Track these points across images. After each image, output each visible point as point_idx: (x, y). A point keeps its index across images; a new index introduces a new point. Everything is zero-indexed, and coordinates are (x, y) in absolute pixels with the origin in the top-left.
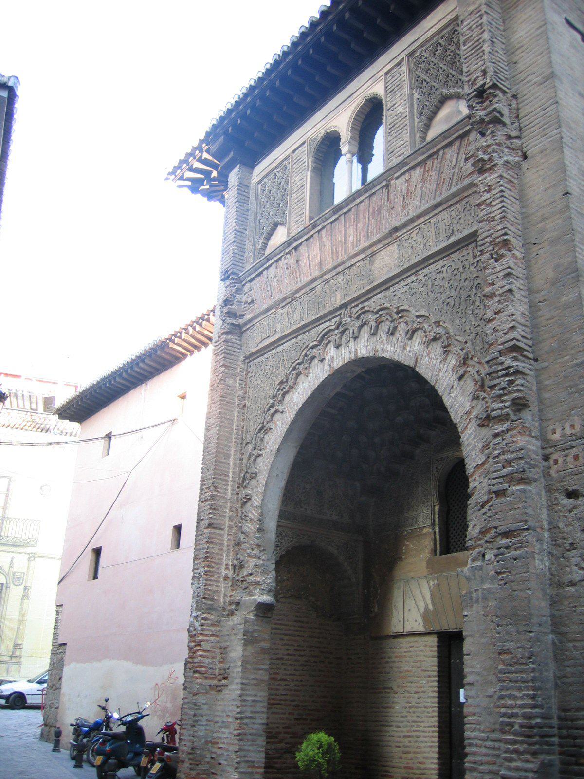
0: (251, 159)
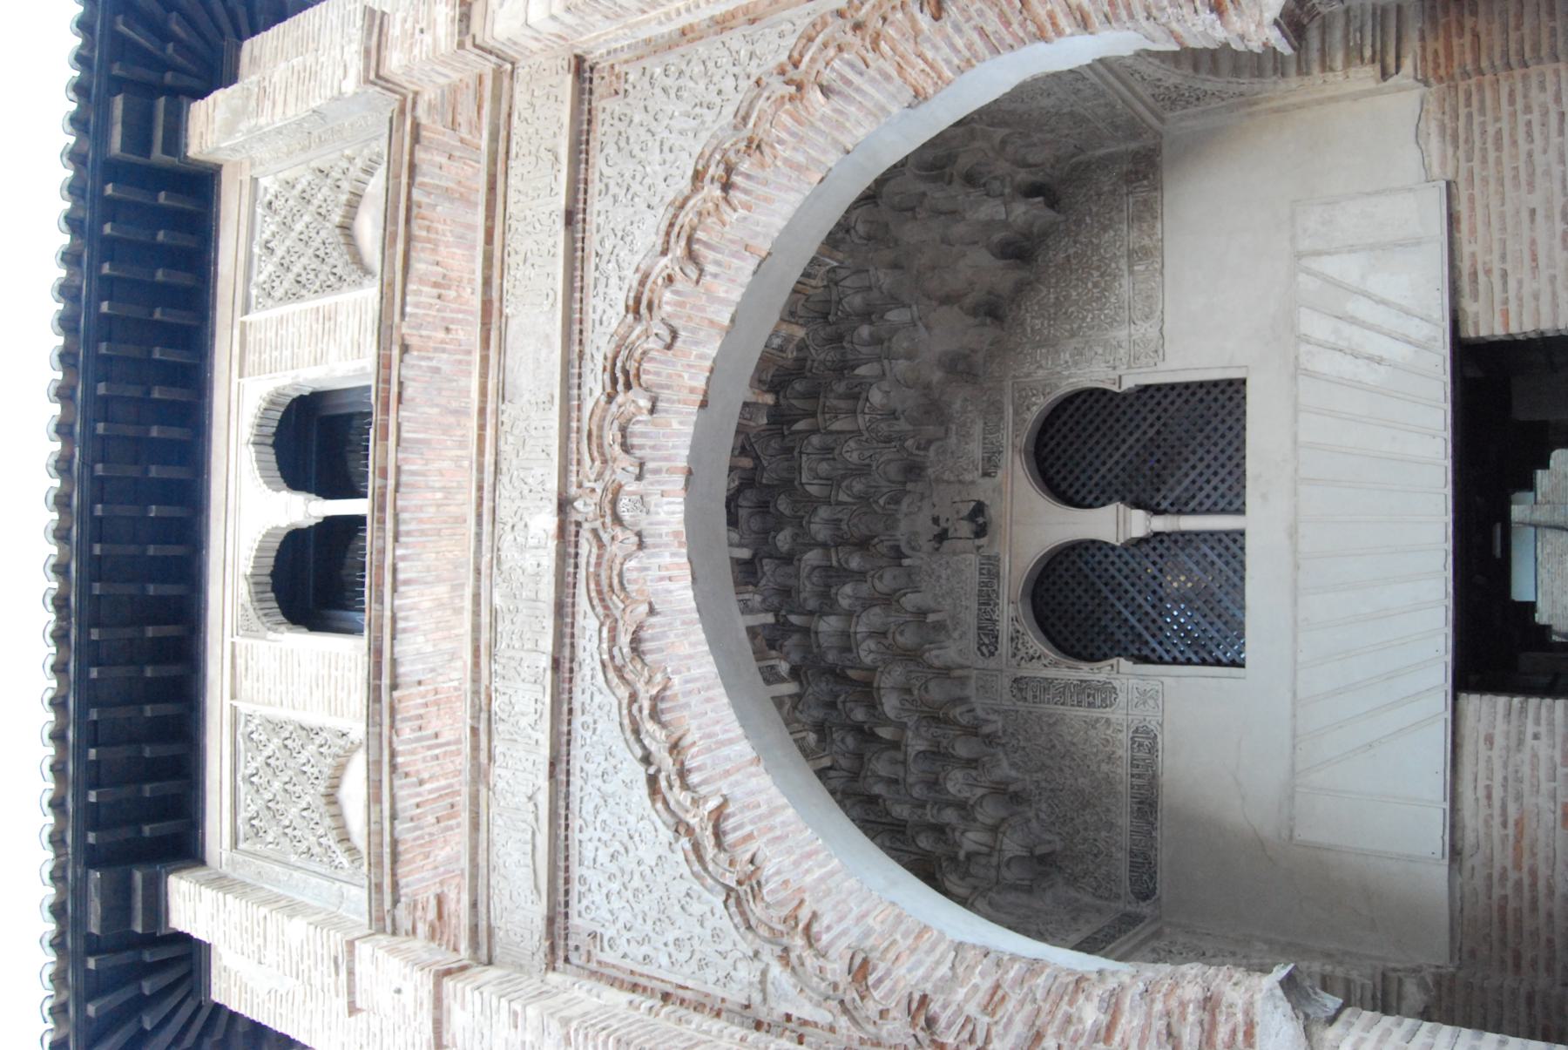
0: (185, 848)
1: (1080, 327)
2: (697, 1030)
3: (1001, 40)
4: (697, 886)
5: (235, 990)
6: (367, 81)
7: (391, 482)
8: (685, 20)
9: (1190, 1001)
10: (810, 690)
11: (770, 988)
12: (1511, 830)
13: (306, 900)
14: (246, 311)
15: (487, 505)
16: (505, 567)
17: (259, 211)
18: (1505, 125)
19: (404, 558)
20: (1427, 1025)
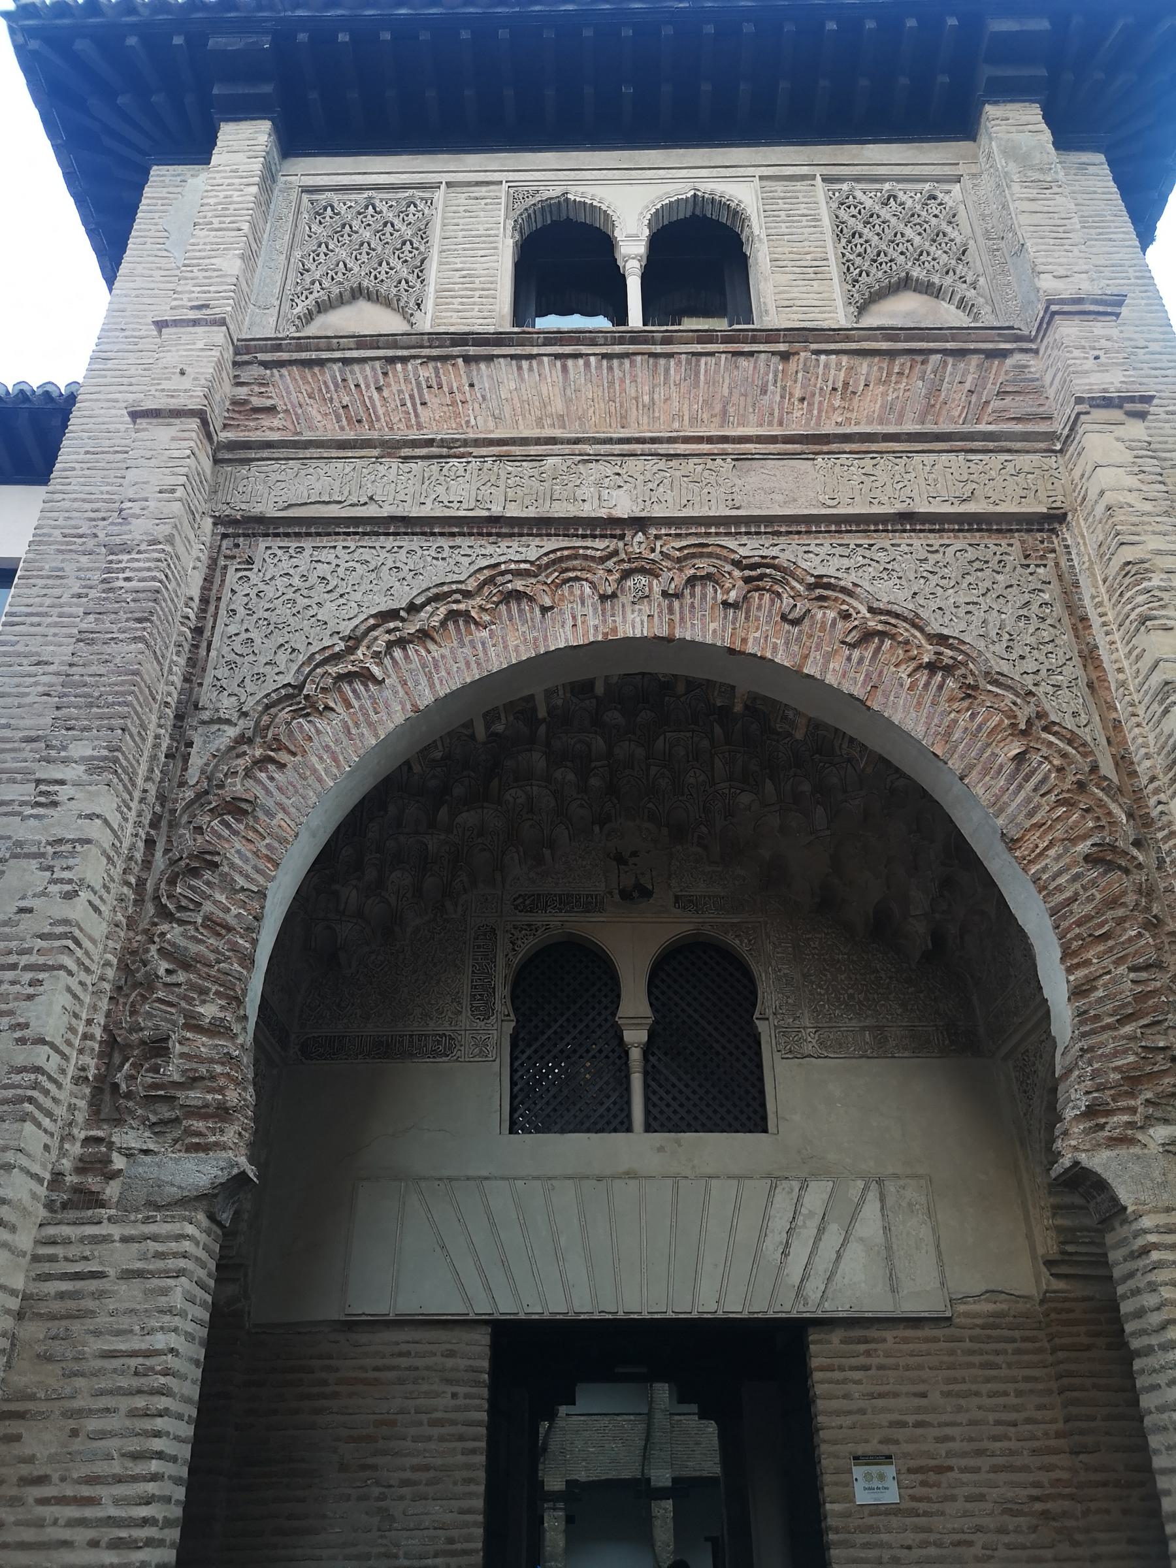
1: (812, 983)
2: (172, 661)
3: (1064, 917)
4: (302, 658)
5: (163, 192)
6: (1050, 302)
7: (658, 349)
8: (1096, 621)
9: (224, 1095)
11: (216, 727)
12: (372, 1375)
13: (258, 271)
14: (826, 179)
15: (638, 448)
16: (580, 466)
17: (927, 186)
18: (1004, 1372)
19: (587, 365)
20: (209, 1299)
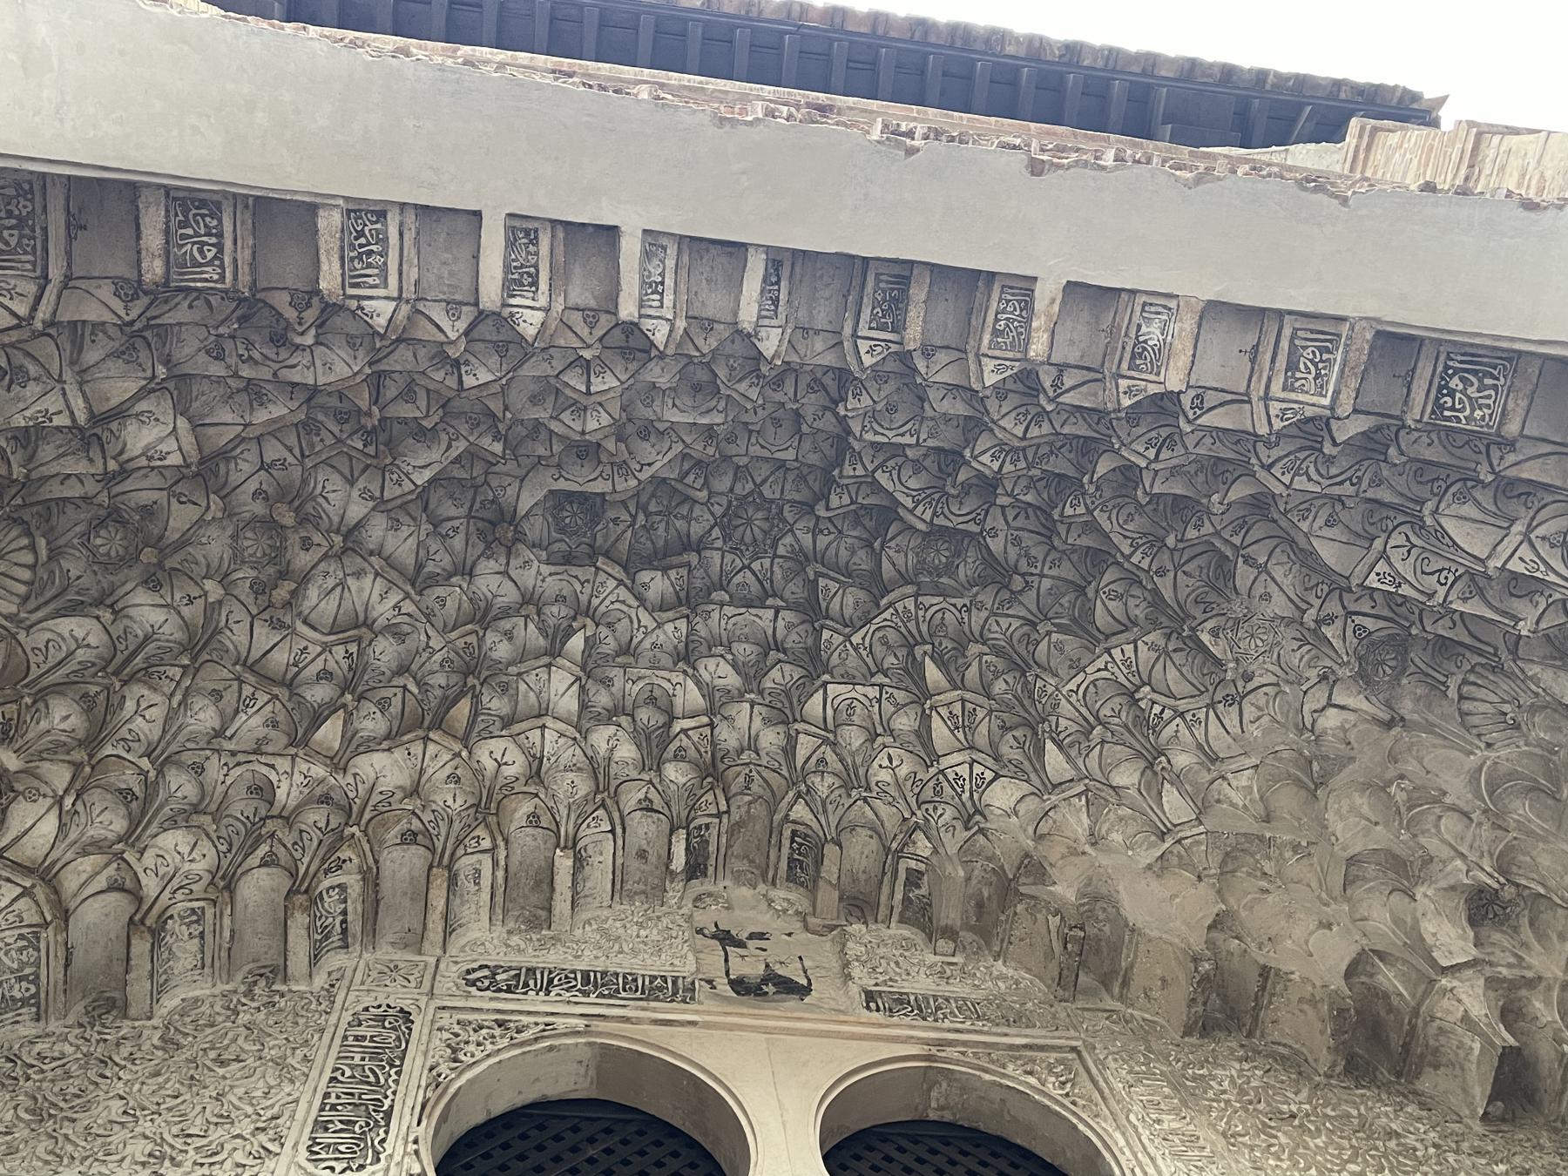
10: (436, 643)
